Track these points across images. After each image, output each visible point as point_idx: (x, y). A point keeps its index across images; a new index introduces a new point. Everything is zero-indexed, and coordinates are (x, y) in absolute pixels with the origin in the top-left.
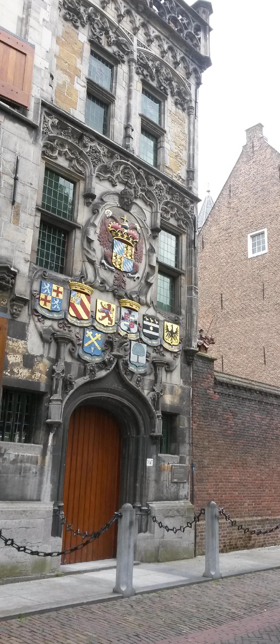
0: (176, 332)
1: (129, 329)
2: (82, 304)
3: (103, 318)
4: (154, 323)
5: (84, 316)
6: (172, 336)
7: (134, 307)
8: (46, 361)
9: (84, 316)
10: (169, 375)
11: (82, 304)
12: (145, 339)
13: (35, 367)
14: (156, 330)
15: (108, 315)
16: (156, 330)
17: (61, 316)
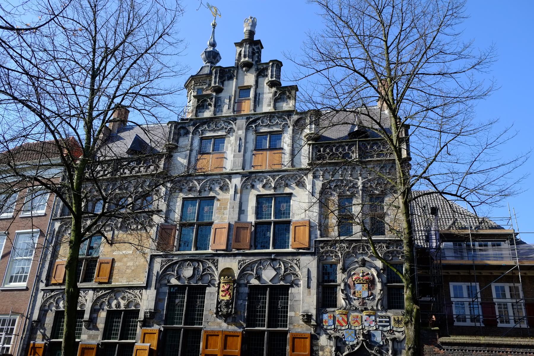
0: (401, 320)
1: (370, 325)
2: (343, 319)
3: (354, 323)
4: (386, 318)
5: (344, 324)
6: (398, 323)
7: (372, 314)
8: (329, 347)
9: (344, 324)
10: (399, 344)
11: (343, 319)
12: (381, 328)
13: (325, 350)
14: (386, 322)
15: (357, 321)
16: (386, 322)
17: (333, 327)
